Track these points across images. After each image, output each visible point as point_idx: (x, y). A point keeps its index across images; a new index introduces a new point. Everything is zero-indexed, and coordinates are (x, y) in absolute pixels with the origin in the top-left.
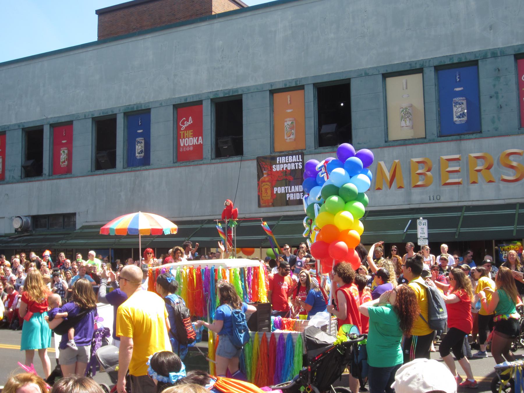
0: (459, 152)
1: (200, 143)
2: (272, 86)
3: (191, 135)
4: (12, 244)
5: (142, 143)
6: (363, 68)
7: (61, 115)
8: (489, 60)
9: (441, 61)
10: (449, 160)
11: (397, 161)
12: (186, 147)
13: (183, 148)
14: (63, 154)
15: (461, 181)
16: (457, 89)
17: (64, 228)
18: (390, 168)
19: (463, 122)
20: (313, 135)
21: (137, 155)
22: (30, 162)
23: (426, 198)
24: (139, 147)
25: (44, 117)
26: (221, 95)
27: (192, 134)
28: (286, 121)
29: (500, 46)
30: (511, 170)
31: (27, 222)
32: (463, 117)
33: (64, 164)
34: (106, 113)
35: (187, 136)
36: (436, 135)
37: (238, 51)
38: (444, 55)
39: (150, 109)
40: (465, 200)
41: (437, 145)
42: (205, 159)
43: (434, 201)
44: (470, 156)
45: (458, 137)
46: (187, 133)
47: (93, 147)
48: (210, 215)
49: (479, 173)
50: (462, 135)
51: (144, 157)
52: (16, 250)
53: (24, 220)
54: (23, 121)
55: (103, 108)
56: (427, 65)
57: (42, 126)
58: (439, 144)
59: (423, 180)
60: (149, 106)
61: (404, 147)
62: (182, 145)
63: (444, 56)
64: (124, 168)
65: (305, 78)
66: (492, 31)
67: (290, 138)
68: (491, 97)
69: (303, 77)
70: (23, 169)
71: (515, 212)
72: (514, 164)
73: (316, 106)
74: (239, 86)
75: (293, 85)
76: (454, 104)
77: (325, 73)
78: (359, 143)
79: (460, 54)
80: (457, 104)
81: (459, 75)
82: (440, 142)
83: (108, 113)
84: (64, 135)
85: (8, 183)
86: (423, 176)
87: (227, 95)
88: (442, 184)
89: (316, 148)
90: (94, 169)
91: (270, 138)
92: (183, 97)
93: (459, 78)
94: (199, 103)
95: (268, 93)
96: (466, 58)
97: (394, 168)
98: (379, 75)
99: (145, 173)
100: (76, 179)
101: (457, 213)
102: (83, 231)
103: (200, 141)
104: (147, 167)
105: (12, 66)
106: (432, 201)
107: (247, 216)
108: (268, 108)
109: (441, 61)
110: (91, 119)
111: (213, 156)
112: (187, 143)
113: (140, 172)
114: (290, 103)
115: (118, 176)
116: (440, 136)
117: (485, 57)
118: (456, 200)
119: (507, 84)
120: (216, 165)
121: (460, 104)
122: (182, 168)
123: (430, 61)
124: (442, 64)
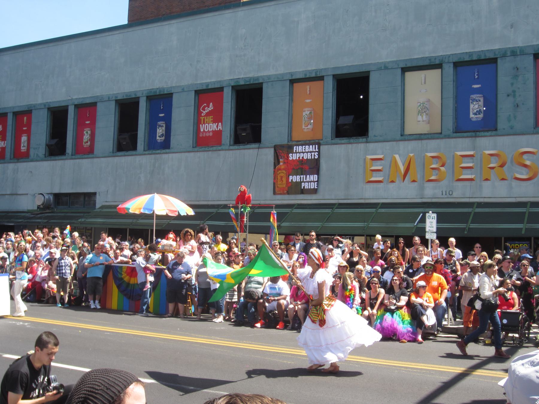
0: (474, 149)
1: (220, 129)
2: (292, 76)
3: (211, 121)
4: (34, 221)
5: (163, 126)
6: (383, 61)
7: (86, 96)
8: (508, 59)
10: (463, 156)
11: (411, 155)
12: (206, 133)
13: (203, 133)
14: (86, 134)
15: (475, 177)
16: (475, 86)
17: (84, 207)
18: (405, 162)
19: (479, 120)
20: (331, 125)
21: (158, 138)
22: (54, 141)
23: (438, 193)
24: (160, 131)
25: (70, 98)
26: (242, 83)
27: (212, 120)
28: (305, 111)
29: (520, 44)
30: (524, 168)
31: (49, 200)
32: (479, 114)
33: (87, 144)
34: (129, 96)
35: (207, 121)
36: (452, 131)
37: (261, 40)
38: (464, 52)
39: (172, 94)
40: (477, 197)
41: (453, 140)
42: (224, 145)
43: (446, 196)
44: (484, 152)
45: (473, 134)
46: (207, 119)
47: (116, 129)
48: (226, 201)
49: (492, 170)
50: (477, 132)
51: (164, 140)
52: (38, 226)
53: (47, 197)
54: (49, 101)
55: (126, 91)
56: (446, 61)
57: (68, 106)
58: (454, 139)
59: (437, 175)
60: (171, 91)
61: (420, 142)
62: (202, 130)
63: (463, 53)
64: (144, 151)
65: (326, 69)
66: (512, 29)
67: (307, 127)
68: (508, 96)
69: (324, 68)
70: (47, 147)
71: (525, 211)
72: (528, 163)
73: (335, 96)
74: (260, 74)
75: (313, 75)
76: (471, 101)
77: (345, 65)
78: (375, 136)
79: (479, 51)
80: (474, 101)
81: (478, 72)
82: (455, 138)
83: (131, 96)
84: (88, 115)
85: (32, 161)
86: (437, 171)
87: (248, 83)
88: (456, 179)
89: (333, 138)
90: (115, 150)
91: (289, 127)
92: (205, 83)
93: (477, 75)
94: (220, 90)
95: (288, 82)
96: (485, 56)
97: (409, 162)
98: (399, 69)
99: (165, 156)
100: (98, 159)
101: (468, 209)
102: (102, 211)
103: (220, 127)
104: (167, 151)
105: (40, 46)
106: (444, 196)
107: (262, 202)
108: (288, 97)
110: (115, 101)
111: (232, 143)
112: (206, 129)
113: (160, 155)
114: (310, 94)
115: (138, 158)
116: (456, 133)
117: (504, 56)
118: (468, 197)
119: (525, 83)
120: (234, 151)
121: (477, 102)
122: (201, 153)
123: (449, 57)
124: (462, 60)
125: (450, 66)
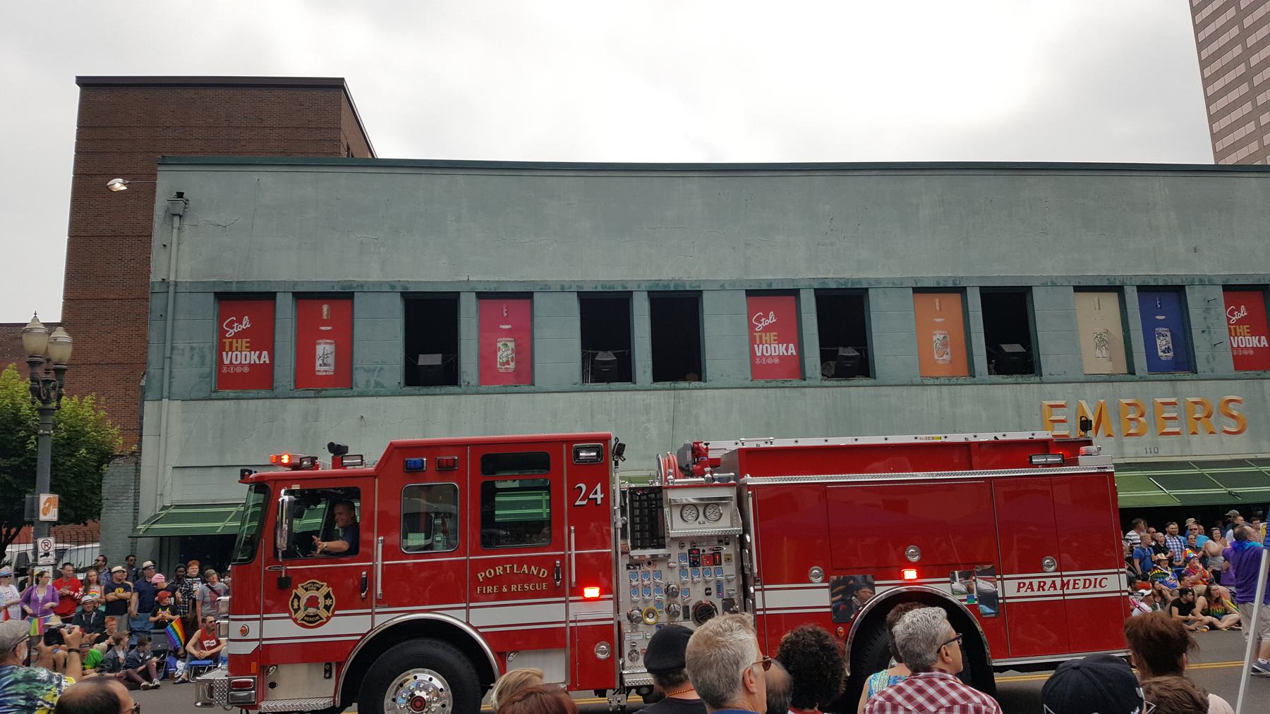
0: (1175, 394)
9: (1144, 281)
42: (811, 378)
81: (1160, 300)
96: (1172, 282)
109: (1144, 281)
114: (940, 310)
125: (1133, 290)
